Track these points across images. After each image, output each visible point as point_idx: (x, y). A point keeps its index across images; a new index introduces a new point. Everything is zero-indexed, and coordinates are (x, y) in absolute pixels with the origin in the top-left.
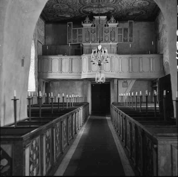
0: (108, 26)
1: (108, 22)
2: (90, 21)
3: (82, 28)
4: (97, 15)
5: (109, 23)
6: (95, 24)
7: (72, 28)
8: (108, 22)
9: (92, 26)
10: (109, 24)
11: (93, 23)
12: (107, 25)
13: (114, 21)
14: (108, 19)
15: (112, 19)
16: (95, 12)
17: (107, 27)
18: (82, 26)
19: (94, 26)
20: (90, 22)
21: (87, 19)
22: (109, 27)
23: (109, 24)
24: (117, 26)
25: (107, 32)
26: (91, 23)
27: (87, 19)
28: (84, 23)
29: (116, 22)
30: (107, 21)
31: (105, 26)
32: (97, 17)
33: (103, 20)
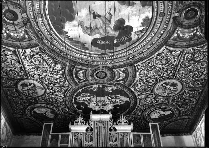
0: (115, 130)
1: (115, 124)
2: (85, 122)
3: (70, 133)
4: (95, 112)
5: (117, 124)
6: (92, 127)
7: (51, 133)
8: (115, 124)
9: (87, 130)
10: (117, 127)
11: (89, 126)
12: (113, 129)
13: (125, 123)
14: (115, 119)
15: (123, 119)
16: (92, 106)
17: (113, 132)
18: (69, 130)
19: (92, 130)
20: (84, 124)
21: (80, 119)
22: (117, 132)
23: (117, 127)
24: (133, 131)
25: (114, 140)
26: (86, 125)
27: (80, 119)
28: (73, 124)
29: (129, 124)
30: (114, 122)
31: (111, 130)
32: (94, 117)
33: (107, 120)
